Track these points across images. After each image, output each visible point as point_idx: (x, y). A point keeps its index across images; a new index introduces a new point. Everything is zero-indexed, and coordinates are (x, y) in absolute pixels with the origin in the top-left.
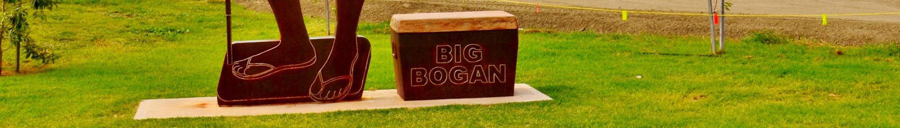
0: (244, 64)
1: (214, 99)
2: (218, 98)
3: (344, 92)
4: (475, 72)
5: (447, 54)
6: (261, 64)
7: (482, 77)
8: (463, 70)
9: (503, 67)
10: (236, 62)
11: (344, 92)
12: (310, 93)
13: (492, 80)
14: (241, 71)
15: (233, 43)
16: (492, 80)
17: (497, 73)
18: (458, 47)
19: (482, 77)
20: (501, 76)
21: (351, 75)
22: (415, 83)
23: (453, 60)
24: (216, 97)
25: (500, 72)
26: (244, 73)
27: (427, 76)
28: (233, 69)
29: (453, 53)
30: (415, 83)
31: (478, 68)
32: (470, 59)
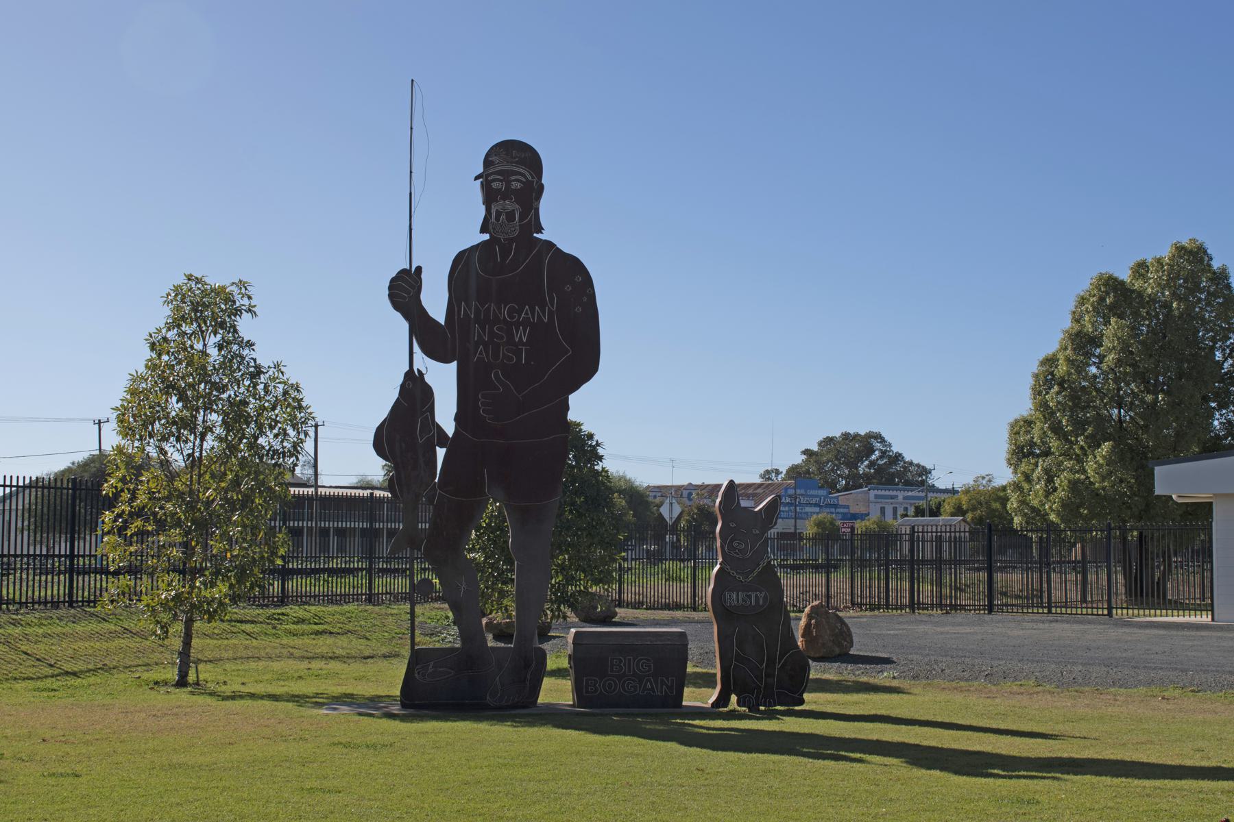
4: (646, 685)
8: (634, 681)
9: (672, 680)
12: (488, 698)
15: (416, 647)
17: (667, 685)
18: (629, 660)
22: (587, 692)
23: (625, 670)
25: (670, 684)
26: (426, 677)
27: (599, 685)
28: (416, 672)
29: (625, 665)
30: (587, 692)
31: (648, 680)
32: (639, 670)
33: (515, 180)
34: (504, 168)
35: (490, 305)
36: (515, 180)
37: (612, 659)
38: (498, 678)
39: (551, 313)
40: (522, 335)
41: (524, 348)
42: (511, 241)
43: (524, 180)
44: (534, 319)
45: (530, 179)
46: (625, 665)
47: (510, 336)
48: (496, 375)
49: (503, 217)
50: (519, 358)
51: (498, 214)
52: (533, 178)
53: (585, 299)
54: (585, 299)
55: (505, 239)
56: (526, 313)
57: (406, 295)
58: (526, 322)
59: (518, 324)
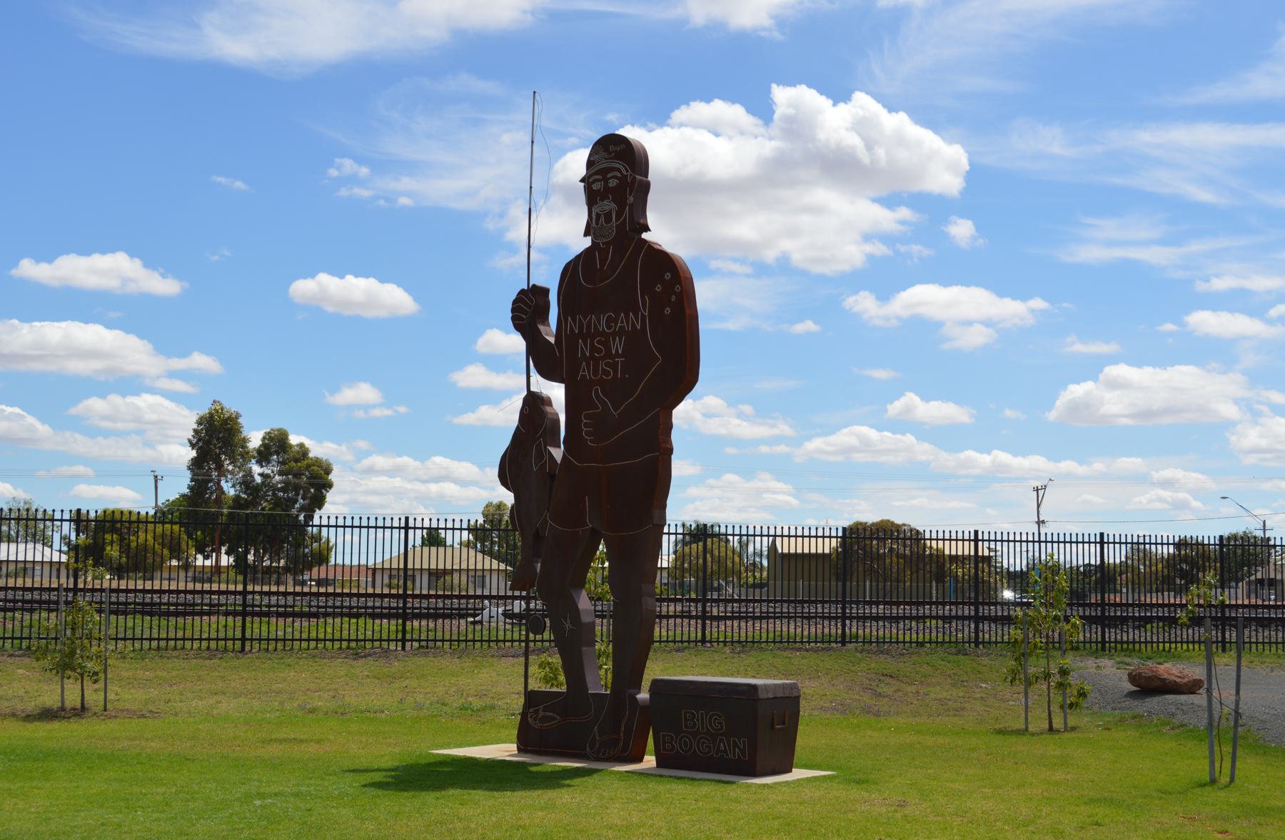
0: (537, 712)
1: (513, 747)
2: (517, 746)
3: (615, 752)
6: (550, 714)
10: (531, 710)
11: (615, 752)
12: (588, 749)
14: (535, 719)
17: (740, 749)
21: (622, 735)
22: (665, 749)
23: (699, 728)
24: (516, 745)
25: (742, 747)
29: (698, 720)
30: (665, 749)
31: (722, 740)
33: (611, 178)
34: (603, 166)
35: (591, 317)
36: (611, 178)
37: (685, 713)
38: (596, 728)
39: (643, 317)
40: (617, 346)
41: (619, 360)
42: (608, 244)
43: (619, 175)
44: (628, 328)
45: (625, 173)
46: (698, 720)
47: (608, 349)
48: (596, 390)
49: (602, 219)
50: (615, 372)
51: (598, 216)
52: (627, 171)
53: (673, 298)
54: (673, 298)
55: (603, 243)
56: (622, 322)
57: (523, 316)
58: (622, 332)
59: (614, 334)
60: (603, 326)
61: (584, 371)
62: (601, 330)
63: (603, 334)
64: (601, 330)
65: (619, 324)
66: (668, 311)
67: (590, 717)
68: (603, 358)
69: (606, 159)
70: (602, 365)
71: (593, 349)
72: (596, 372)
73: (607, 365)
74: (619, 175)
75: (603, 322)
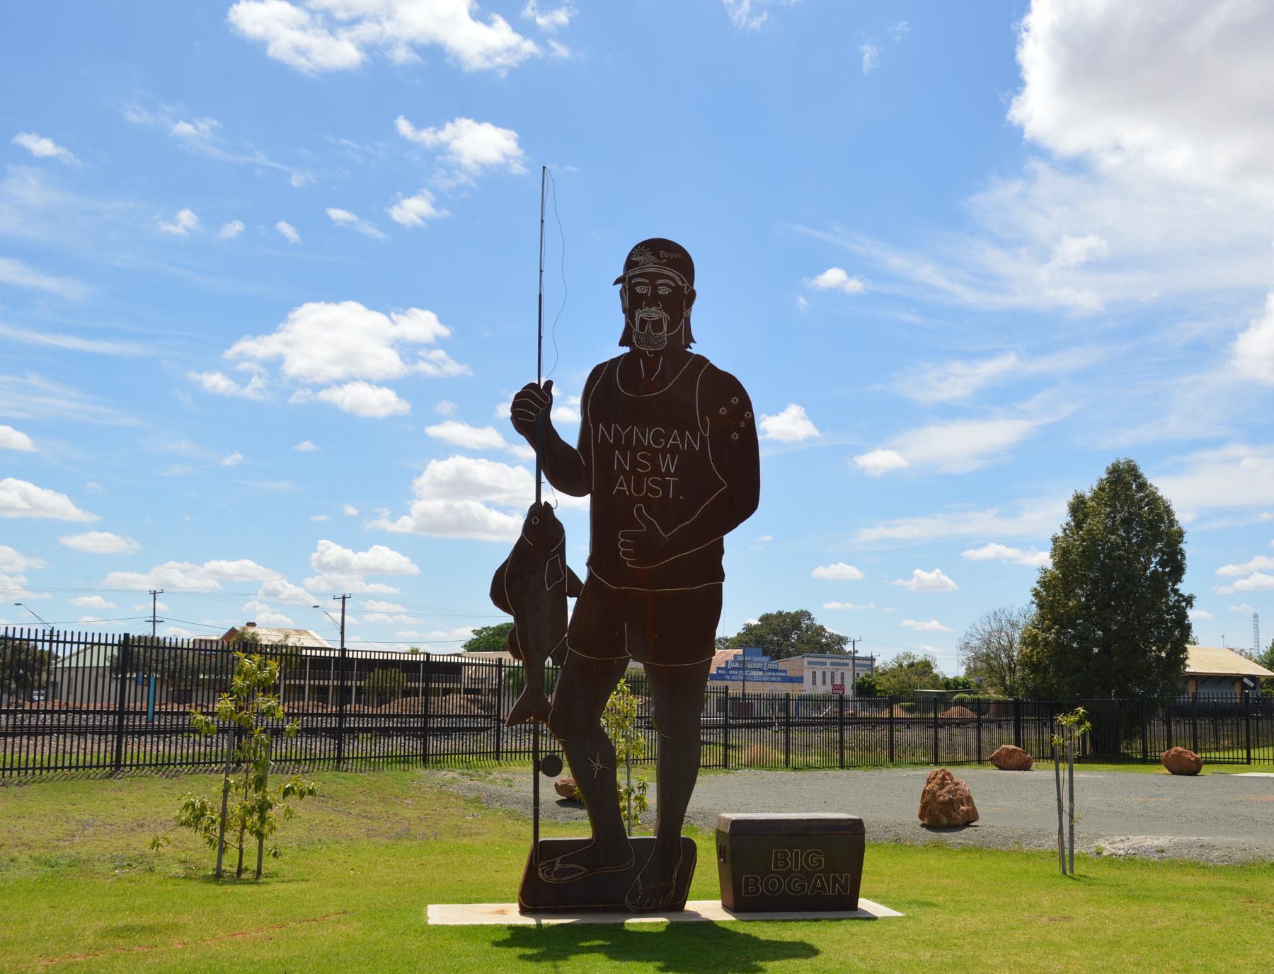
3: (665, 902)
4: (816, 882)
5: (784, 860)
6: (571, 866)
7: (823, 888)
8: (802, 878)
9: (846, 877)
10: (543, 863)
11: (665, 902)
12: (626, 901)
13: (834, 891)
14: (549, 874)
15: (540, 840)
16: (834, 891)
18: (797, 852)
19: (823, 888)
20: (844, 887)
22: (747, 892)
26: (552, 876)
27: (761, 884)
29: (791, 859)
30: (747, 892)
32: (810, 867)
33: (661, 285)
36: (661, 285)
38: (639, 876)
39: (703, 439)
40: (668, 464)
41: (672, 479)
42: (657, 354)
43: (673, 285)
44: (683, 446)
45: (680, 284)
46: (791, 859)
47: (656, 467)
49: (648, 326)
50: (666, 491)
51: (643, 322)
52: (683, 282)
53: (743, 424)
54: (743, 424)
55: (650, 352)
57: (533, 414)
58: (674, 450)
59: (664, 452)
60: (648, 440)
61: (621, 485)
62: (646, 444)
63: (649, 448)
64: (646, 444)
65: (671, 442)
66: (735, 436)
67: (629, 865)
68: (648, 475)
69: (654, 264)
70: (647, 482)
71: (634, 463)
72: (638, 488)
73: (654, 482)
74: (674, 285)
75: (650, 435)
